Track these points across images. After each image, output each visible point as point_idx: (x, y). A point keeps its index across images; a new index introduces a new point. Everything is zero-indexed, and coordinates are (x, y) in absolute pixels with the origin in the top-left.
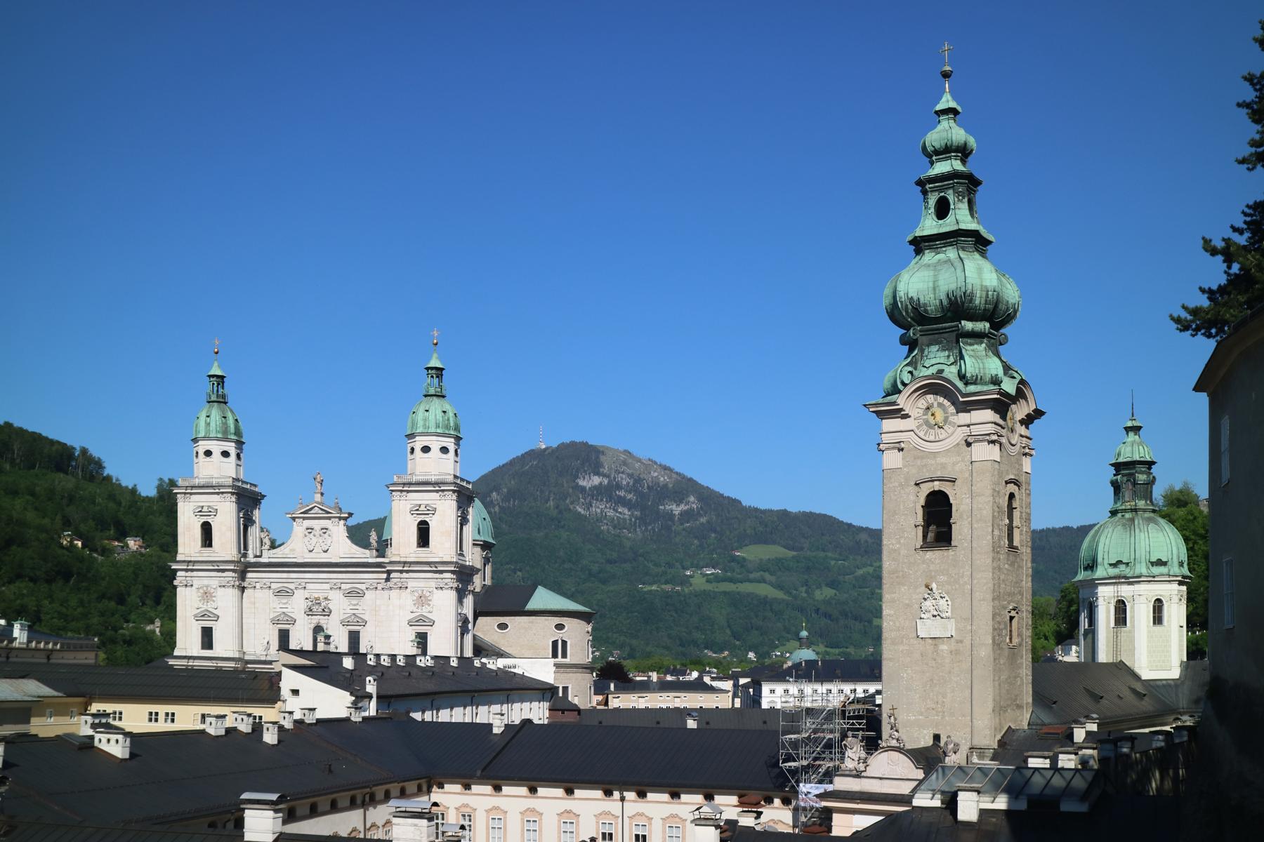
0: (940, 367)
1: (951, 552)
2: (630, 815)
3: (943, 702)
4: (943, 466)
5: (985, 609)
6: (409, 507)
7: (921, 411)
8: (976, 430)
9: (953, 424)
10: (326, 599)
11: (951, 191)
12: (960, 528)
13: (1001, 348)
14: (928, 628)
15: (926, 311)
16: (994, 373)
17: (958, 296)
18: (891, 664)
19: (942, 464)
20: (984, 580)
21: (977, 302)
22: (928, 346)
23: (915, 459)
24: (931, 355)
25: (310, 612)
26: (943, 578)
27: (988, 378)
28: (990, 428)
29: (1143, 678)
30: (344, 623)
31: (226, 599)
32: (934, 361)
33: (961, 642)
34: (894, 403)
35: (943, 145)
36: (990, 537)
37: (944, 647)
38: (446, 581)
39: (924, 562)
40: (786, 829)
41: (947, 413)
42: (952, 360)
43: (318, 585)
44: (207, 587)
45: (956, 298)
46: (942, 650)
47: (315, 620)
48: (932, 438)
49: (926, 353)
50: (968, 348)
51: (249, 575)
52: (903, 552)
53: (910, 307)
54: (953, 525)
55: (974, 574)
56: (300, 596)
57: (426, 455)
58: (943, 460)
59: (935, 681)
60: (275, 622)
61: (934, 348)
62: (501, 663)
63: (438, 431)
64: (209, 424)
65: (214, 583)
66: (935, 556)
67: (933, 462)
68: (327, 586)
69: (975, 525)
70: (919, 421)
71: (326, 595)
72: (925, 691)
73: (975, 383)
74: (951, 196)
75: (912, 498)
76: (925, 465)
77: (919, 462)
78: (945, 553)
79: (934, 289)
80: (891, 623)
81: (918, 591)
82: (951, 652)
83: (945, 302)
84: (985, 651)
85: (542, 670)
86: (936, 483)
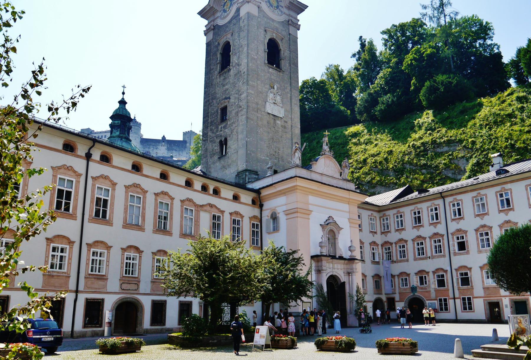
1: (281, 74)
2: (94, 176)
3: (279, 152)
9: (281, 12)
14: (270, 108)
18: (252, 122)
19: (276, 27)
33: (286, 122)
37: (278, 122)
39: (268, 72)
46: (278, 124)
52: (259, 62)
55: (292, 89)
58: (277, 25)
59: (274, 140)
69: (292, 66)
72: (269, 144)
80: (252, 98)
81: (266, 86)
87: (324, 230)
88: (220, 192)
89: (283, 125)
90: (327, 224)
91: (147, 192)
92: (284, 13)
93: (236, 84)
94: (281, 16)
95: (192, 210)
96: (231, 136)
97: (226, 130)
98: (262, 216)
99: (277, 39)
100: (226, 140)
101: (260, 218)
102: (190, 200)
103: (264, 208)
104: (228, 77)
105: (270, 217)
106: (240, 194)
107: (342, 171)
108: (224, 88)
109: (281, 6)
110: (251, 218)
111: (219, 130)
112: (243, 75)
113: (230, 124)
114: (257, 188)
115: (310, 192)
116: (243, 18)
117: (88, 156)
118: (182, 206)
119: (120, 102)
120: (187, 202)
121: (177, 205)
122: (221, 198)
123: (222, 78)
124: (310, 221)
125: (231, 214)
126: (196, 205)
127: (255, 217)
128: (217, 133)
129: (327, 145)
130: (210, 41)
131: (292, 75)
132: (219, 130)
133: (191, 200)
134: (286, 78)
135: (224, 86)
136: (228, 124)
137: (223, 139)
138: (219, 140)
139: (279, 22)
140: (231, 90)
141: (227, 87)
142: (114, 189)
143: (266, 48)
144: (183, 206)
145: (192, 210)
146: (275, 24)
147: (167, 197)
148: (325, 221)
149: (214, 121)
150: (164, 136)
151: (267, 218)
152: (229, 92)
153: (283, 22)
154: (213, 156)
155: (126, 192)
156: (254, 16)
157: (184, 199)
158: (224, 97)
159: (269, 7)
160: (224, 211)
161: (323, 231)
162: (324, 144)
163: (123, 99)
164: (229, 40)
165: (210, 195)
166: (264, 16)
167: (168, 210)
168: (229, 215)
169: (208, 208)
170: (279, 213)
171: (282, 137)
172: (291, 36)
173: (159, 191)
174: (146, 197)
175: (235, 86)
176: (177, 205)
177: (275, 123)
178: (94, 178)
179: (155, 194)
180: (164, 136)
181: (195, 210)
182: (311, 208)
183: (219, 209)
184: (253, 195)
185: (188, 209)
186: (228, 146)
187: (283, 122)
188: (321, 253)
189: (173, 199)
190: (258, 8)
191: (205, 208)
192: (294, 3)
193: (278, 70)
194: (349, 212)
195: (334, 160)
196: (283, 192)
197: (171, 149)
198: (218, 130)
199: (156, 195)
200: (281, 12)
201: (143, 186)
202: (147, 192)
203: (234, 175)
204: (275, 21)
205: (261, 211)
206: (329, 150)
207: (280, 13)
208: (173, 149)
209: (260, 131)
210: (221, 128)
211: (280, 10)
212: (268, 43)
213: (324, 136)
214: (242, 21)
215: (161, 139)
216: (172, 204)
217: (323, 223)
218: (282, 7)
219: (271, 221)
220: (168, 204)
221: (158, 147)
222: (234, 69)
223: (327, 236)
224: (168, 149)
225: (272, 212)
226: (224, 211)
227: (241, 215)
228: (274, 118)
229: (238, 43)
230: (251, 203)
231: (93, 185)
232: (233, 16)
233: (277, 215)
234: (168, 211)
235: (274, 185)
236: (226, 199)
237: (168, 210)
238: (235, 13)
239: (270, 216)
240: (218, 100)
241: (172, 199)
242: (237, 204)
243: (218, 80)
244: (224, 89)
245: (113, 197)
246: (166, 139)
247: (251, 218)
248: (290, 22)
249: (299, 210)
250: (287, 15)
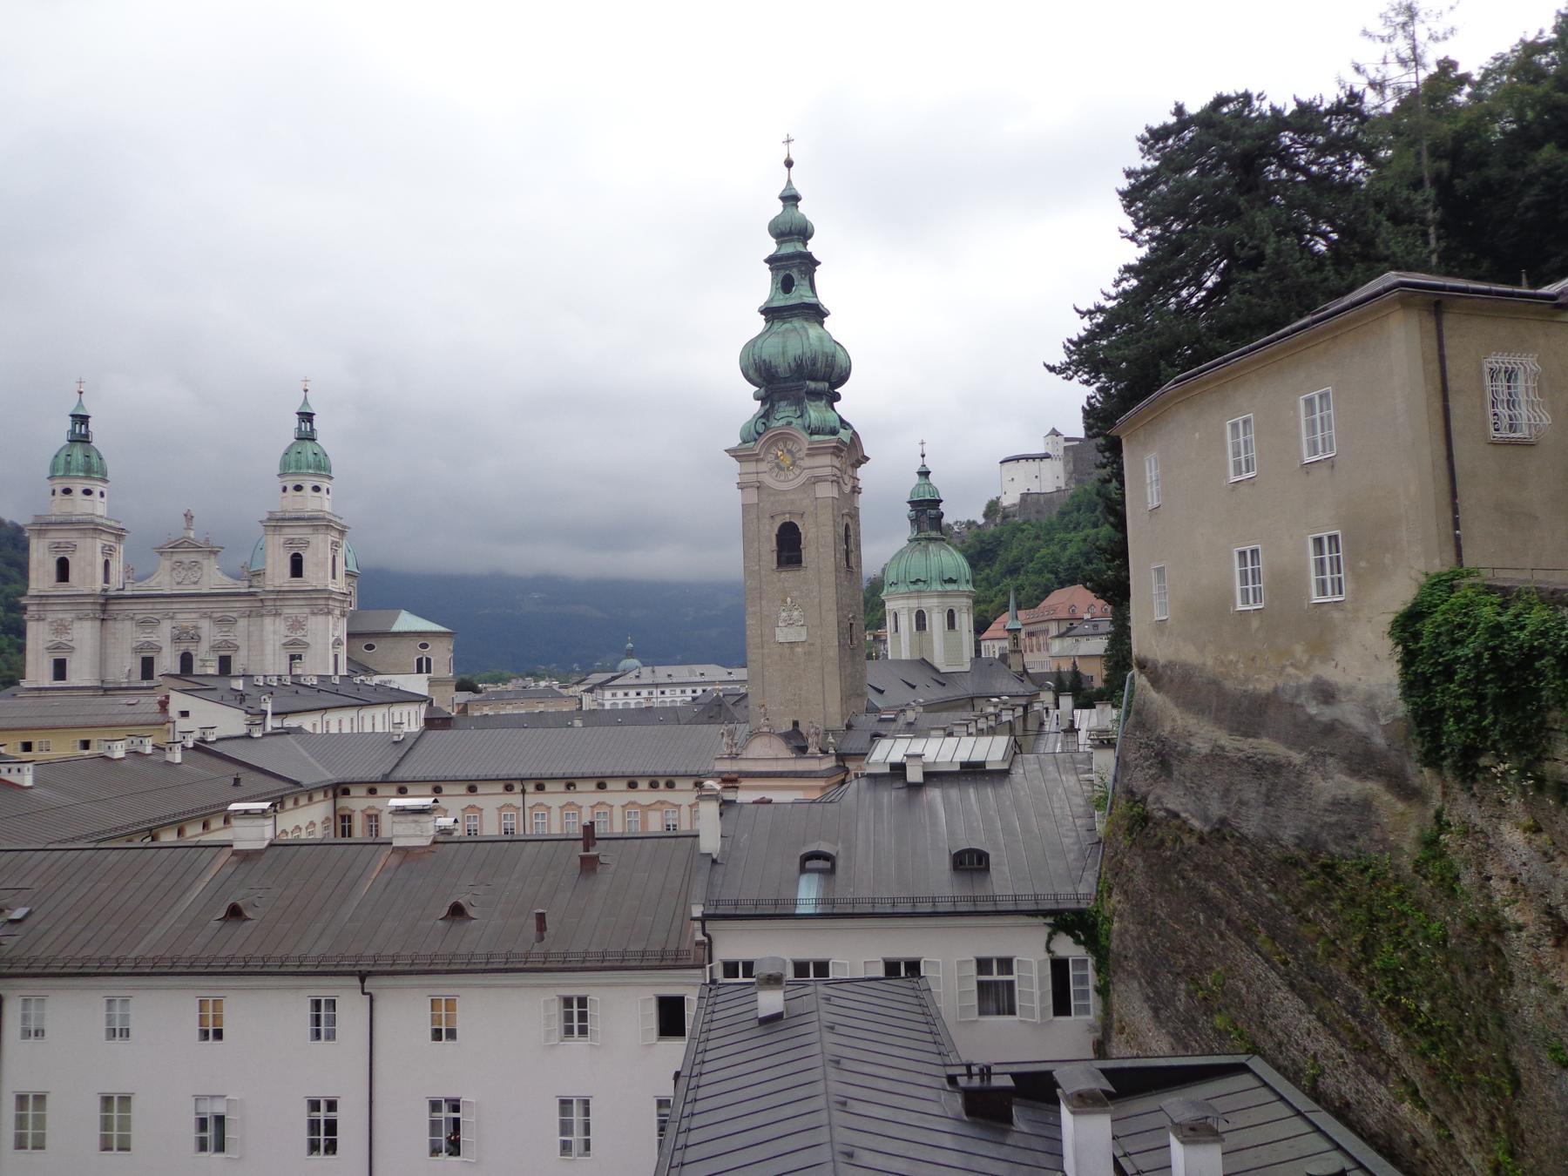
0: (790, 419)
4: (792, 502)
5: (832, 618)
6: (282, 540)
8: (819, 472)
10: (196, 627)
11: (795, 270)
12: (808, 554)
13: (835, 404)
14: (783, 635)
15: (777, 372)
16: (832, 425)
20: (830, 594)
21: (819, 365)
22: (778, 401)
24: (781, 409)
25: (177, 639)
26: (795, 593)
27: (828, 429)
28: (828, 471)
29: (942, 671)
30: (214, 648)
31: (84, 634)
32: (783, 415)
33: (813, 644)
34: (752, 449)
35: (788, 227)
36: (833, 560)
37: (799, 650)
38: (321, 607)
42: (799, 413)
43: (187, 617)
44: (62, 620)
47: (183, 647)
48: (782, 478)
49: (776, 407)
50: (812, 404)
51: (110, 607)
52: (763, 572)
54: (803, 551)
56: (166, 628)
57: (298, 493)
60: (137, 650)
61: (783, 404)
62: (376, 679)
63: (310, 471)
64: (70, 462)
65: (68, 616)
66: (788, 576)
68: (194, 616)
69: (821, 550)
71: (194, 624)
73: (817, 433)
74: (795, 274)
75: (768, 527)
77: (772, 498)
78: (797, 573)
79: (783, 353)
83: (793, 365)
84: (833, 652)
85: (417, 684)
86: (788, 516)
102: (633, 803)
109: (799, 459)
117: (524, 792)
121: (617, 812)
126: (641, 806)
142: (549, 813)
155: (561, 813)
169: (658, 806)
176: (617, 812)
178: (531, 808)
191: (653, 807)
199: (593, 807)
201: (577, 802)
207: (798, 471)
218: (802, 459)
231: (531, 814)
236: (682, 790)
245: (549, 819)
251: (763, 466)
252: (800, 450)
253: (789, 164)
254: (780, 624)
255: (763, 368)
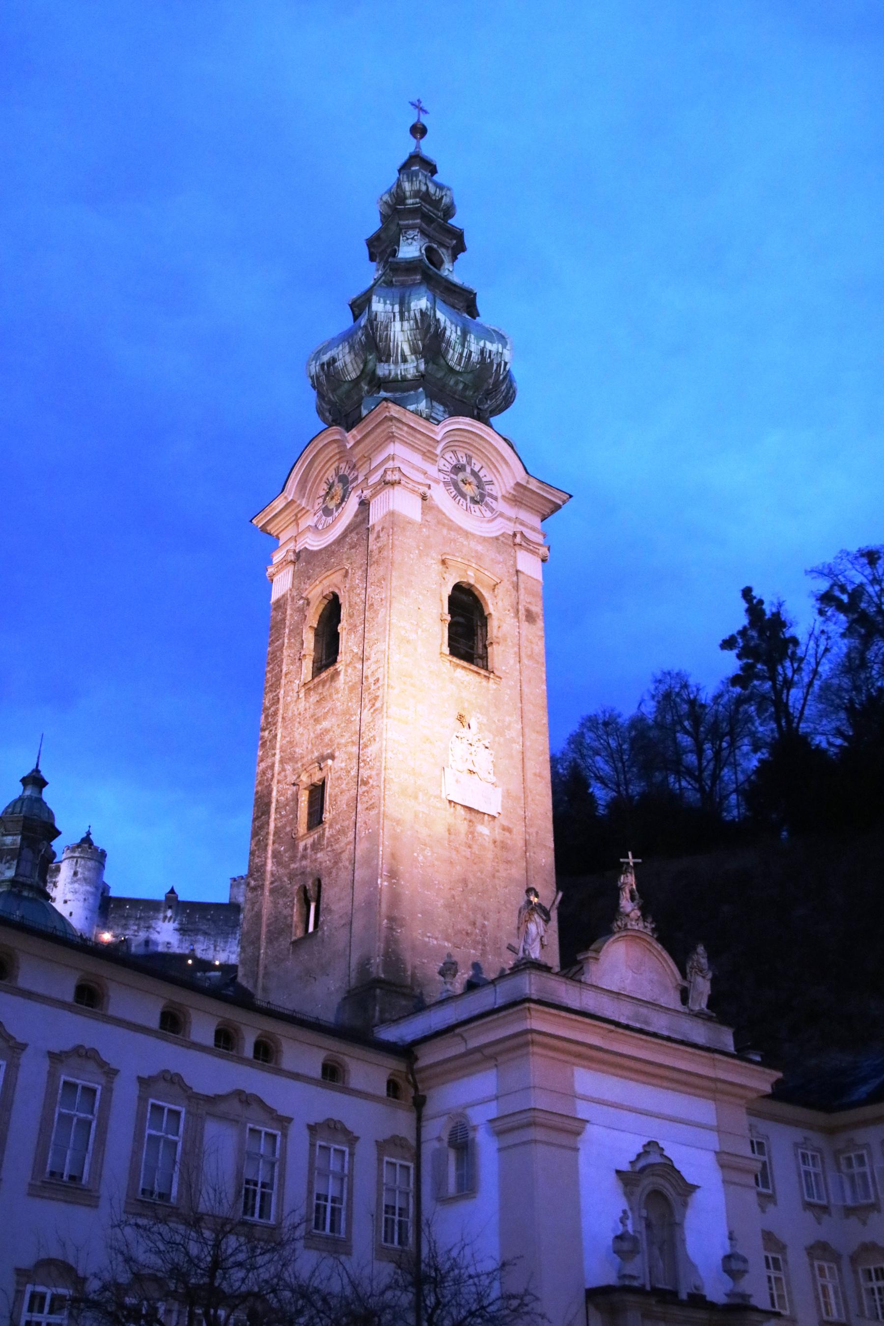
1: (492, 685)
3: (484, 926)
7: (448, 467)
9: (492, 510)
11: (444, 250)
15: (447, 351)
17: (495, 362)
19: (476, 552)
23: (439, 522)
37: (483, 829)
39: (452, 680)
40: (265, 1124)
41: (483, 489)
45: (492, 361)
46: (481, 834)
53: (432, 330)
58: (480, 548)
59: (470, 886)
67: (465, 543)
69: (525, 661)
70: (446, 477)
76: (454, 540)
82: (495, 842)
83: (475, 357)
87: (632, 1193)
88: (279, 1051)
89: (498, 838)
90: (643, 1170)
91: (23, 1047)
92: (501, 515)
93: (352, 715)
94: (493, 520)
95: (178, 1113)
96: (334, 871)
97: (319, 855)
98: (423, 1139)
99: (478, 586)
100: (319, 883)
101: (413, 1142)
102: (172, 1079)
103: (429, 1109)
104: (331, 695)
105: (445, 1143)
106: (346, 1059)
107: (685, 984)
108: (319, 727)
109: (491, 496)
110: (382, 1146)
111: (299, 855)
112: (373, 687)
113: (332, 836)
114: (409, 1038)
115: (579, 1056)
116: (377, 528)
118: (142, 1099)
119: (25, 781)
120: (162, 1086)
122: (279, 1072)
123: (314, 698)
124: (582, 1156)
125: (312, 1129)
126: (193, 1097)
127: (394, 1143)
128: (293, 866)
129: (633, 899)
130: (283, 596)
131: (526, 689)
132: (299, 855)
133: (176, 1079)
134: (507, 698)
135: (317, 721)
136: (327, 834)
137: (310, 884)
138: (296, 887)
139: (485, 539)
140: (338, 731)
141: (325, 724)
143: (446, 610)
144: (146, 1101)
145: (178, 1113)
146: (473, 544)
147: (91, 1066)
148: (633, 1157)
149: (284, 826)
150: (172, 891)
151: (436, 1145)
152: (331, 740)
153: (497, 538)
154: (277, 939)
156: (410, 522)
157: (154, 1073)
158: (316, 754)
159: (454, 498)
160: (290, 1120)
161: (628, 1195)
162: (625, 896)
163: (37, 771)
164: (337, 591)
165: (242, 1060)
166: (439, 522)
167: (92, 1113)
168: (306, 1132)
169: (235, 1106)
170: (474, 1128)
171: (494, 876)
172: (521, 577)
173: (68, 1047)
174: (17, 1066)
175: (349, 722)
177: (472, 833)
179: (51, 1055)
180: (172, 891)
181: (188, 1113)
182: (583, 1110)
183: (270, 1111)
184: (393, 1065)
185: (162, 1108)
186: (323, 906)
187: (498, 830)
188: (622, 1277)
189: (116, 1072)
190: (424, 498)
191: (223, 1107)
192: (530, 486)
193: (482, 672)
194: (718, 1130)
195: (659, 947)
196: (488, 1052)
197: (191, 931)
198: (295, 857)
199: (55, 1057)
200: (492, 510)
202: (23, 1047)
203: (337, 999)
204: (473, 535)
205: (419, 1119)
206: (639, 914)
207: (488, 514)
208: (197, 931)
209: (425, 857)
210: (305, 849)
211: (487, 505)
212: (450, 598)
213: (621, 869)
214: (375, 535)
215: (163, 898)
216: (108, 1090)
217: (625, 1167)
218: (496, 499)
219: (452, 1155)
220: (93, 1091)
221: (153, 923)
222: (350, 670)
223: (644, 1213)
224: (182, 930)
225: (453, 1124)
226: (290, 1120)
227: (346, 1132)
228: (468, 816)
229: (363, 597)
230: (382, 1091)
232: (350, 525)
233: (471, 1135)
234: (90, 1117)
235: (458, 1031)
236: (296, 1076)
237: (92, 1113)
238: (356, 516)
239: (446, 1137)
240: (299, 764)
241: (111, 1073)
242: (337, 1096)
243: (302, 704)
244: (319, 732)
246: (180, 898)
247: (382, 1146)
248: (518, 539)
249: (541, 1118)
250: (509, 519)
251: (432, 470)
252: (491, 483)
253: (419, 131)
254: (451, 762)
255: (432, 330)
